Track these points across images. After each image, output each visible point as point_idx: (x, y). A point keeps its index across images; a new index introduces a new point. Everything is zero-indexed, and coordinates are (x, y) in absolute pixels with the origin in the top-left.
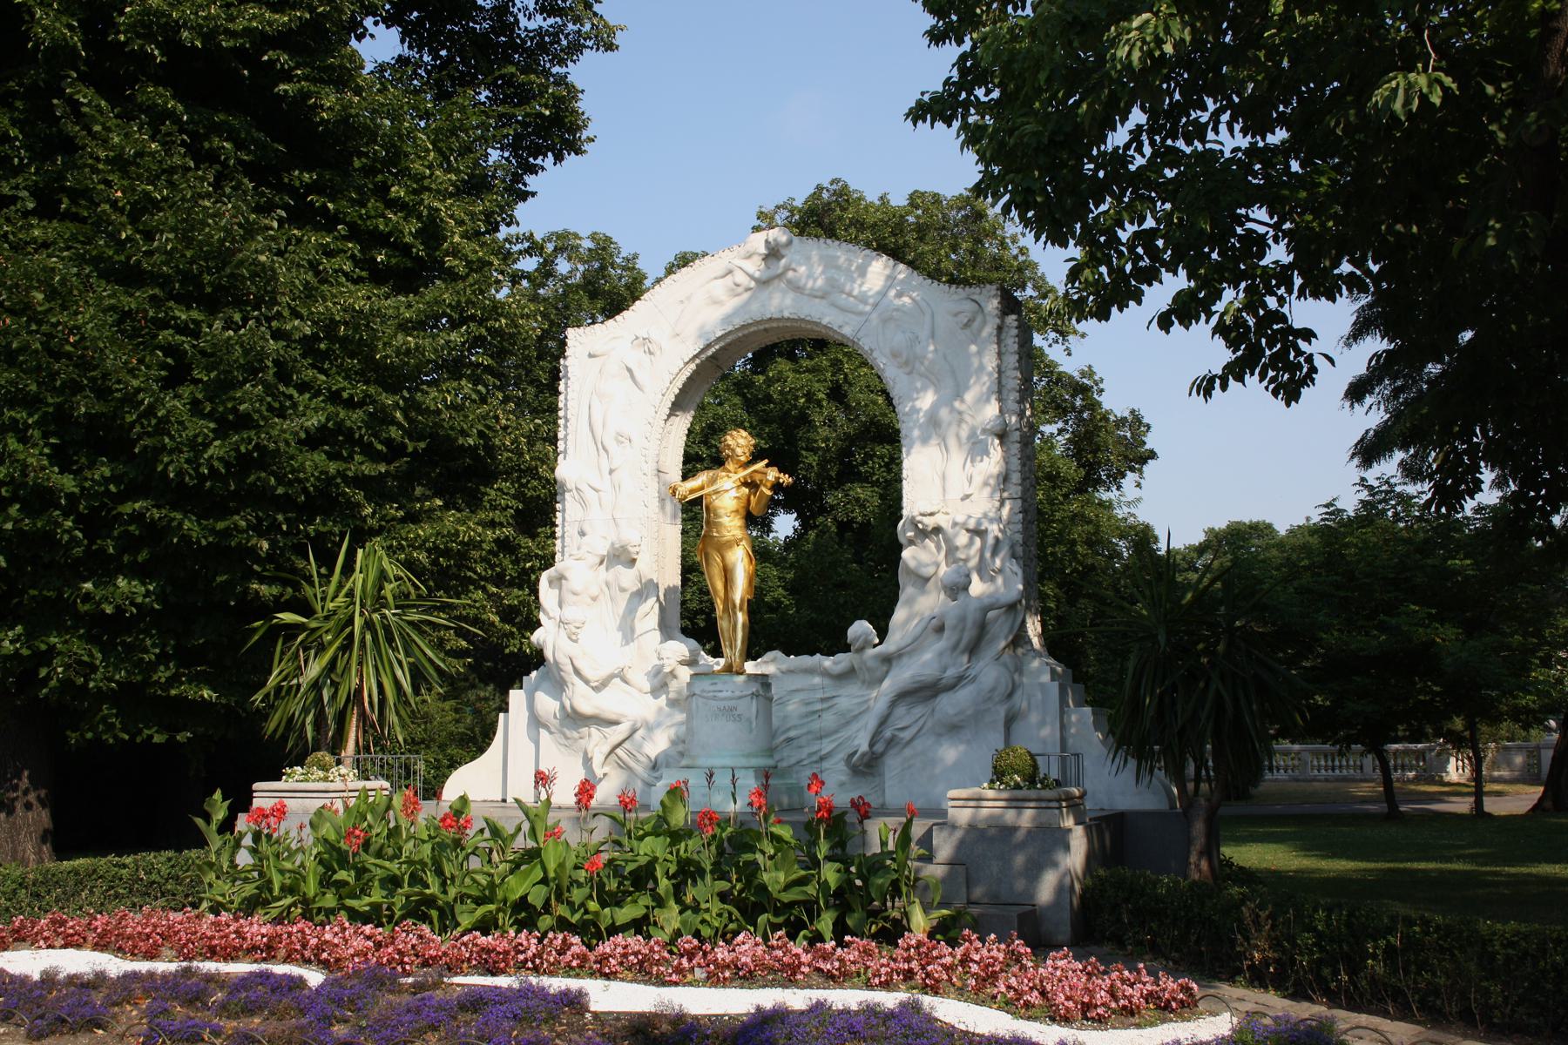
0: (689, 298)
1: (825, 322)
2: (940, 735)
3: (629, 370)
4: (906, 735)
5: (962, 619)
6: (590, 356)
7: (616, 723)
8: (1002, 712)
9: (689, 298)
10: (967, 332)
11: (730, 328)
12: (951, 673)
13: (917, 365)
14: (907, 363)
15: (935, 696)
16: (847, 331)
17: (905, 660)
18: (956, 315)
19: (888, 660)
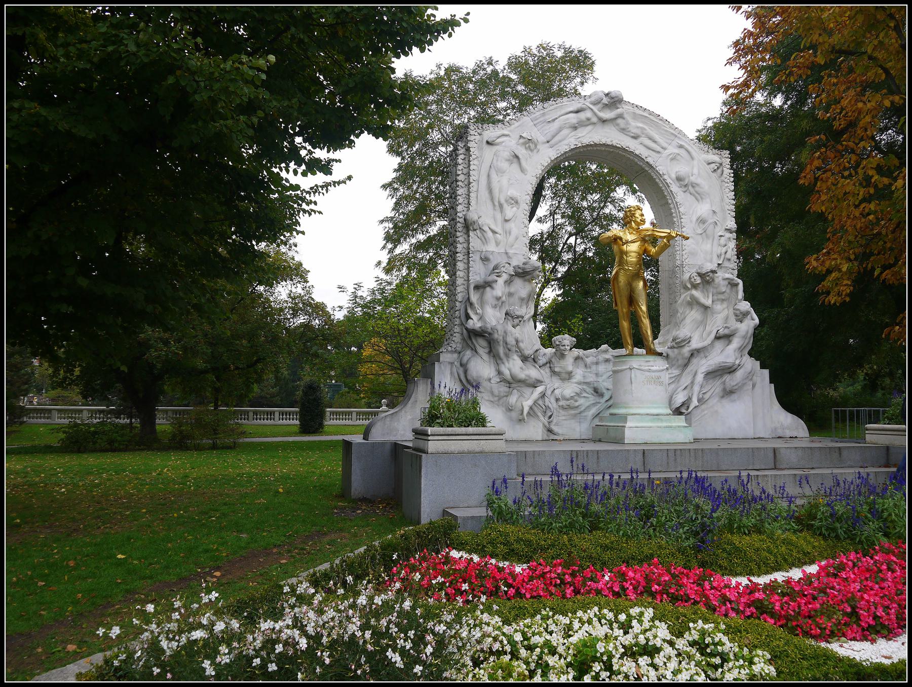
0: (554, 120)
1: (637, 152)
2: (723, 397)
3: (517, 157)
4: (707, 396)
5: (747, 332)
6: (488, 143)
7: (534, 385)
8: (751, 383)
9: (554, 120)
10: (714, 174)
11: (580, 145)
12: (737, 362)
13: (690, 187)
14: (686, 186)
15: (721, 376)
16: (649, 160)
17: (702, 355)
18: (709, 164)
19: (694, 353)
